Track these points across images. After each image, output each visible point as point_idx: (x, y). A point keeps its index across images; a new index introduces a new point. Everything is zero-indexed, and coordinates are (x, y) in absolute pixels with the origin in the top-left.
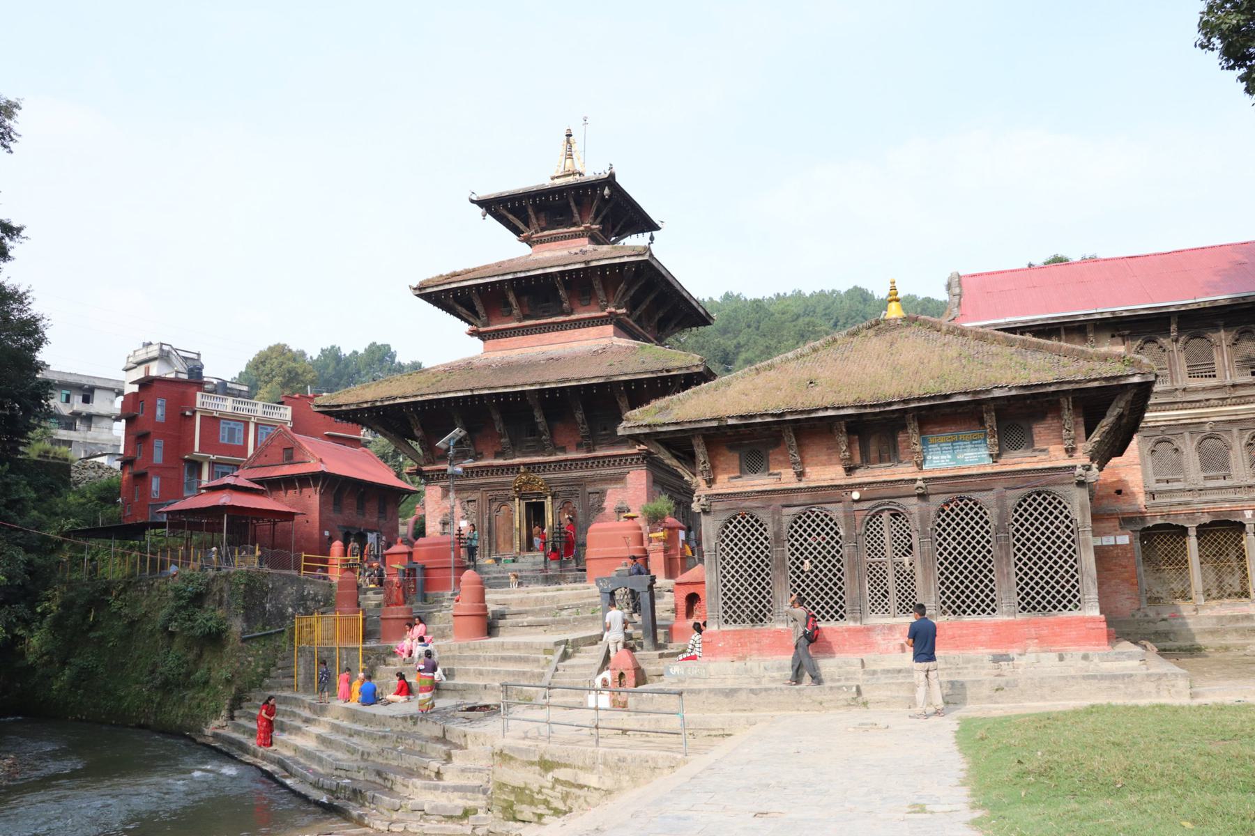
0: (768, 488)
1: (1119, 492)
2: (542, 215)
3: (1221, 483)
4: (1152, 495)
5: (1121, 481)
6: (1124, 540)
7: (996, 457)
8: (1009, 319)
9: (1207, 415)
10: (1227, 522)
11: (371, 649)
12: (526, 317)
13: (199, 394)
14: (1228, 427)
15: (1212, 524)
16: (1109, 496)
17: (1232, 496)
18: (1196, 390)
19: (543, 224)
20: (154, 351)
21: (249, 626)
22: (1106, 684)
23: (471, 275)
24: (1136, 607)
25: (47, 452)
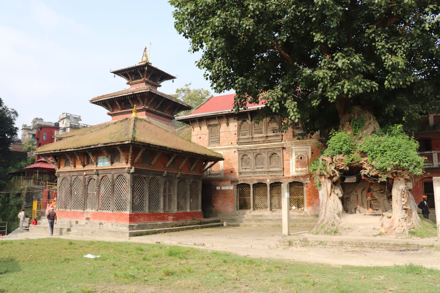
0: (69, 170)
1: (232, 172)
2: (133, 76)
3: (261, 170)
4: (240, 173)
5: (233, 168)
6: (231, 188)
7: (112, 163)
8: (200, 114)
9: (257, 147)
10: (262, 183)
11: (40, 211)
12: (122, 109)
13: (56, 131)
14: (264, 151)
15: (258, 183)
16: (228, 173)
17: (264, 175)
18: (256, 138)
19: (133, 78)
20: (65, 116)
21: (27, 204)
22: (113, 233)
23: (108, 96)
24: (233, 210)
25: (30, 148)
